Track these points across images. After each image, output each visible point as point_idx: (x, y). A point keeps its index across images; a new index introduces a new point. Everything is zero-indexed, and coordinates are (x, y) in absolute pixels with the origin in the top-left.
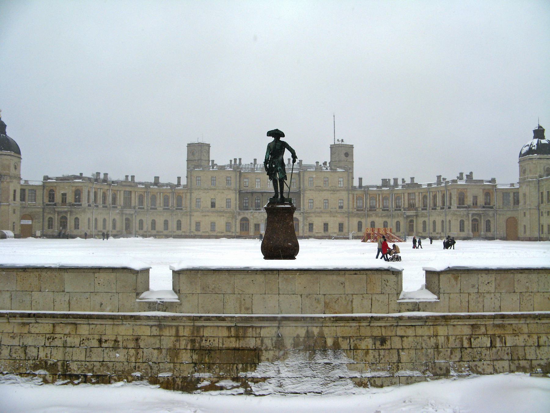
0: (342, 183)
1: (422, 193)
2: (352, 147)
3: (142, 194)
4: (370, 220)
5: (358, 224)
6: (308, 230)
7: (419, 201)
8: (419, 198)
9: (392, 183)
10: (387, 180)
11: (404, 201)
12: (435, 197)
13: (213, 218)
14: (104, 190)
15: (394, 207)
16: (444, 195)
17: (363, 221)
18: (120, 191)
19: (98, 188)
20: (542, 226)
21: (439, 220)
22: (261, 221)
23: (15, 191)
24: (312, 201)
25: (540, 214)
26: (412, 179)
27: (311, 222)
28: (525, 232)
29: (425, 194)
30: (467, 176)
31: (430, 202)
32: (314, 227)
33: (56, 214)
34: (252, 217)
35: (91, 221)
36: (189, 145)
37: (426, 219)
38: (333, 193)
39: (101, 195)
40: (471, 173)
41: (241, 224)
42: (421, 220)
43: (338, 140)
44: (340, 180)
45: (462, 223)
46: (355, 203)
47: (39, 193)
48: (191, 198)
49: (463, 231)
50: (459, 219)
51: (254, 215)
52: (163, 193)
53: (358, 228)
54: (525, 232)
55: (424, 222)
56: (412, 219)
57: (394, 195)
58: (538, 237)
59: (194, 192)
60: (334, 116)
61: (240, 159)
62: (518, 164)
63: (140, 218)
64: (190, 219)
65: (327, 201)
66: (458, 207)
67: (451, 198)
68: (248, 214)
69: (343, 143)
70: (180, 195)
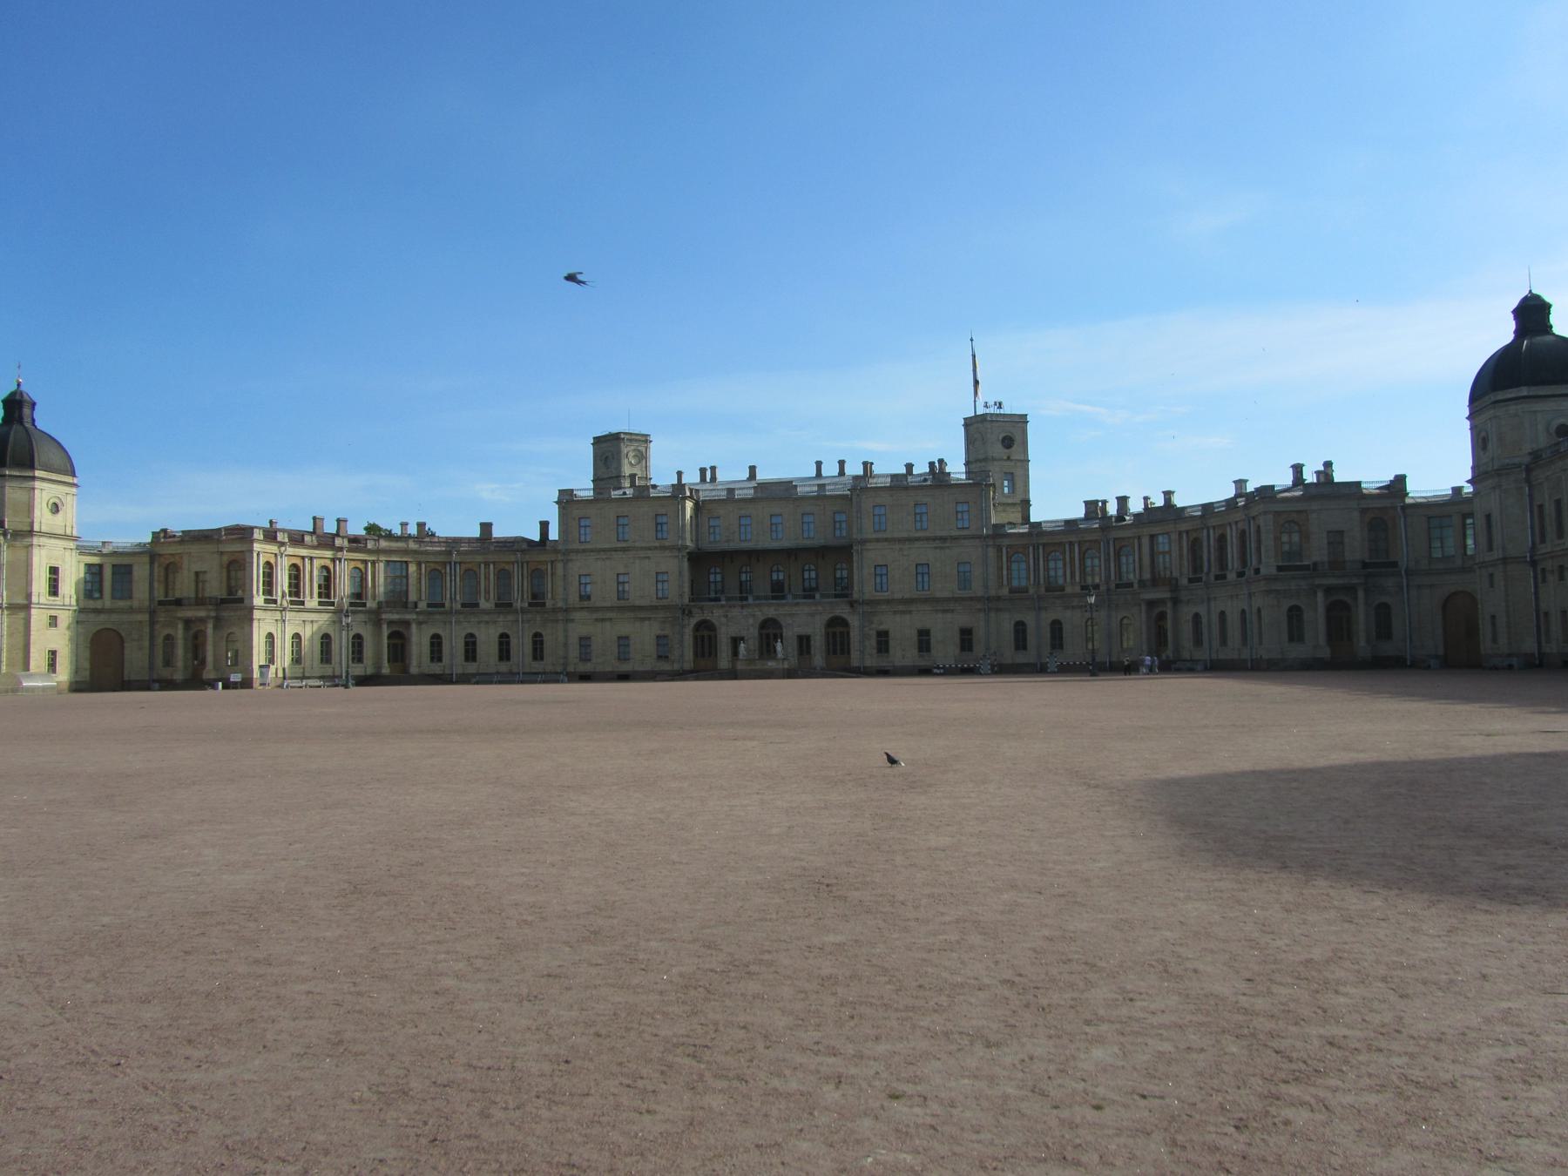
0: (966, 516)
1: (1187, 532)
2: (1023, 420)
3: (440, 568)
4: (1048, 617)
5: (1016, 631)
6: (875, 651)
7: (1181, 556)
8: (1181, 548)
9: (1112, 509)
10: (1100, 504)
11: (1140, 559)
12: (1222, 539)
13: (625, 627)
14: (323, 562)
15: (1113, 577)
16: (1243, 532)
17: (1029, 619)
18: (374, 563)
19: (303, 558)
20: (1546, 614)
21: (1233, 609)
22: (748, 629)
23: (54, 571)
24: (881, 570)
25: (1539, 576)
26: (1168, 495)
27: (882, 627)
28: (1495, 640)
29: (1195, 535)
30: (1318, 473)
31: (1208, 553)
32: (891, 643)
33: (180, 626)
34: (723, 620)
35: (278, 643)
36: (598, 441)
37: (1202, 610)
38: (940, 545)
39: (316, 573)
40: (1328, 465)
41: (695, 638)
42: (1187, 612)
43: (986, 406)
44: (960, 509)
45: (1295, 614)
46: (1005, 572)
47: (141, 572)
48: (565, 576)
49: (1301, 639)
50: (1287, 604)
51: (730, 615)
52: (494, 563)
53: (1016, 639)
54: (1495, 640)
55: (1197, 617)
56: (1161, 609)
57: (1111, 543)
58: (1533, 655)
59: (574, 558)
60: (972, 340)
61: (713, 469)
62: (1467, 424)
63: (433, 631)
64: (566, 631)
65: (926, 570)
66: (1280, 569)
67: (1259, 542)
68: (715, 615)
69: (1002, 412)
70: (539, 567)
